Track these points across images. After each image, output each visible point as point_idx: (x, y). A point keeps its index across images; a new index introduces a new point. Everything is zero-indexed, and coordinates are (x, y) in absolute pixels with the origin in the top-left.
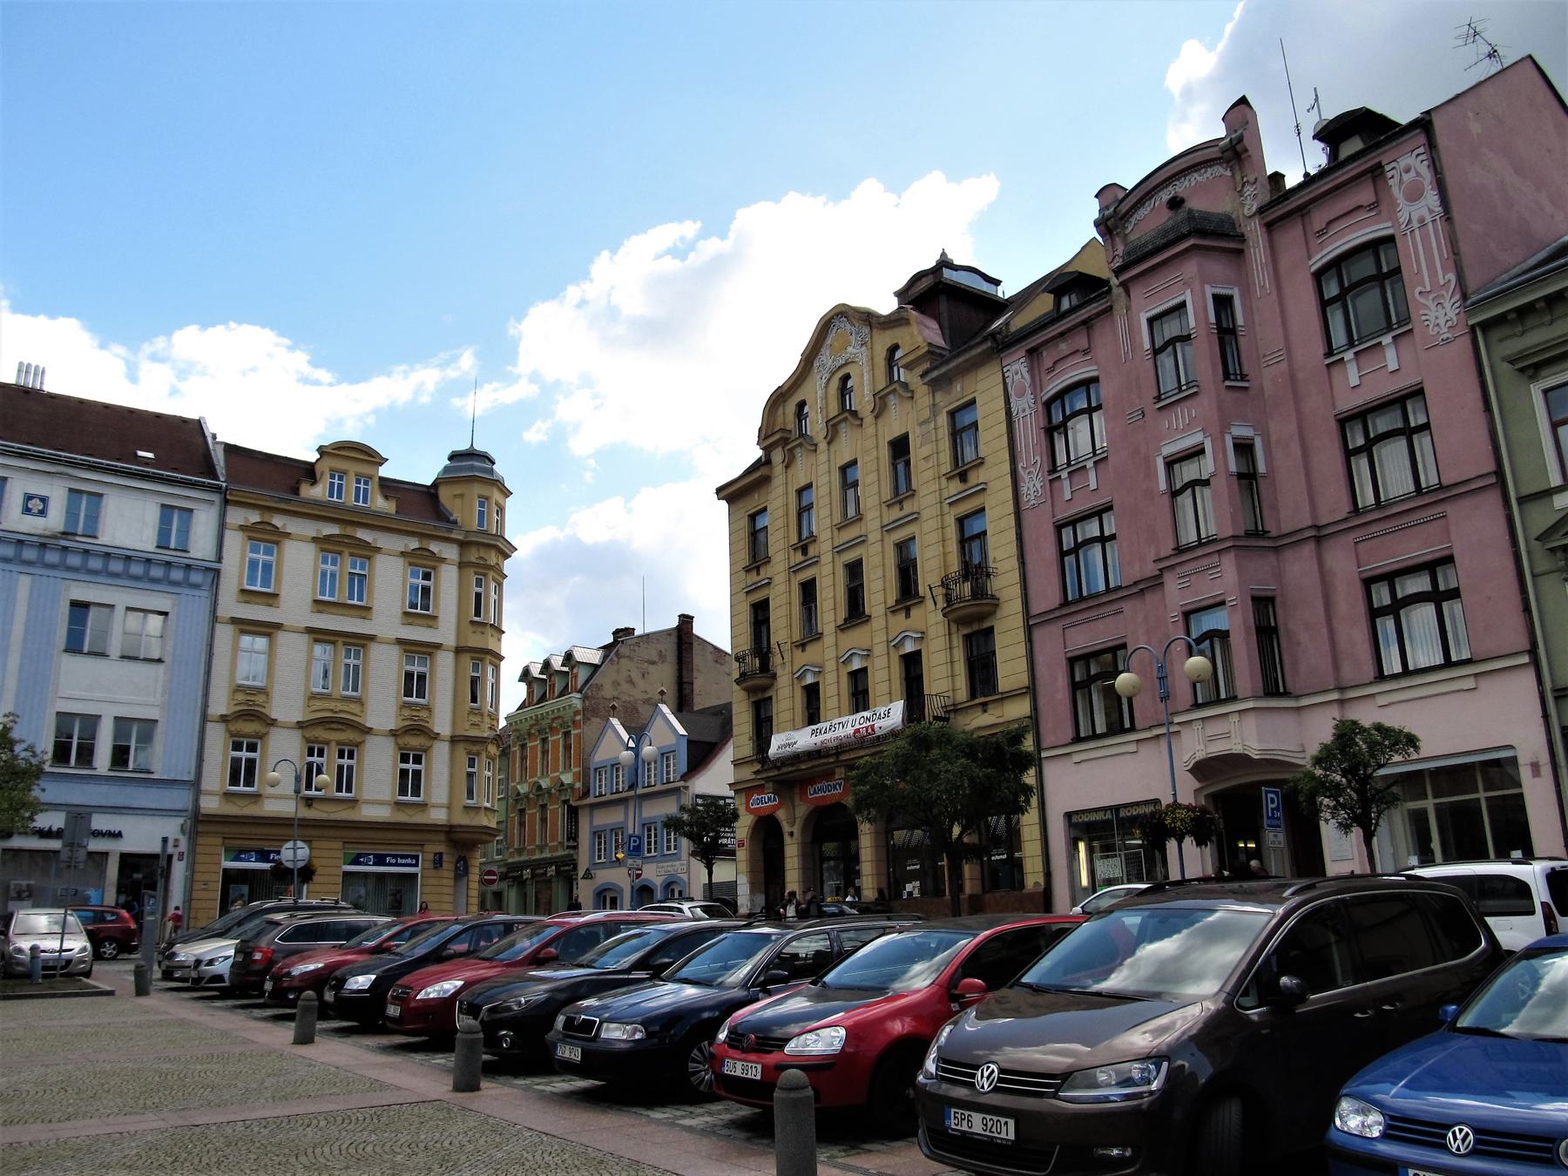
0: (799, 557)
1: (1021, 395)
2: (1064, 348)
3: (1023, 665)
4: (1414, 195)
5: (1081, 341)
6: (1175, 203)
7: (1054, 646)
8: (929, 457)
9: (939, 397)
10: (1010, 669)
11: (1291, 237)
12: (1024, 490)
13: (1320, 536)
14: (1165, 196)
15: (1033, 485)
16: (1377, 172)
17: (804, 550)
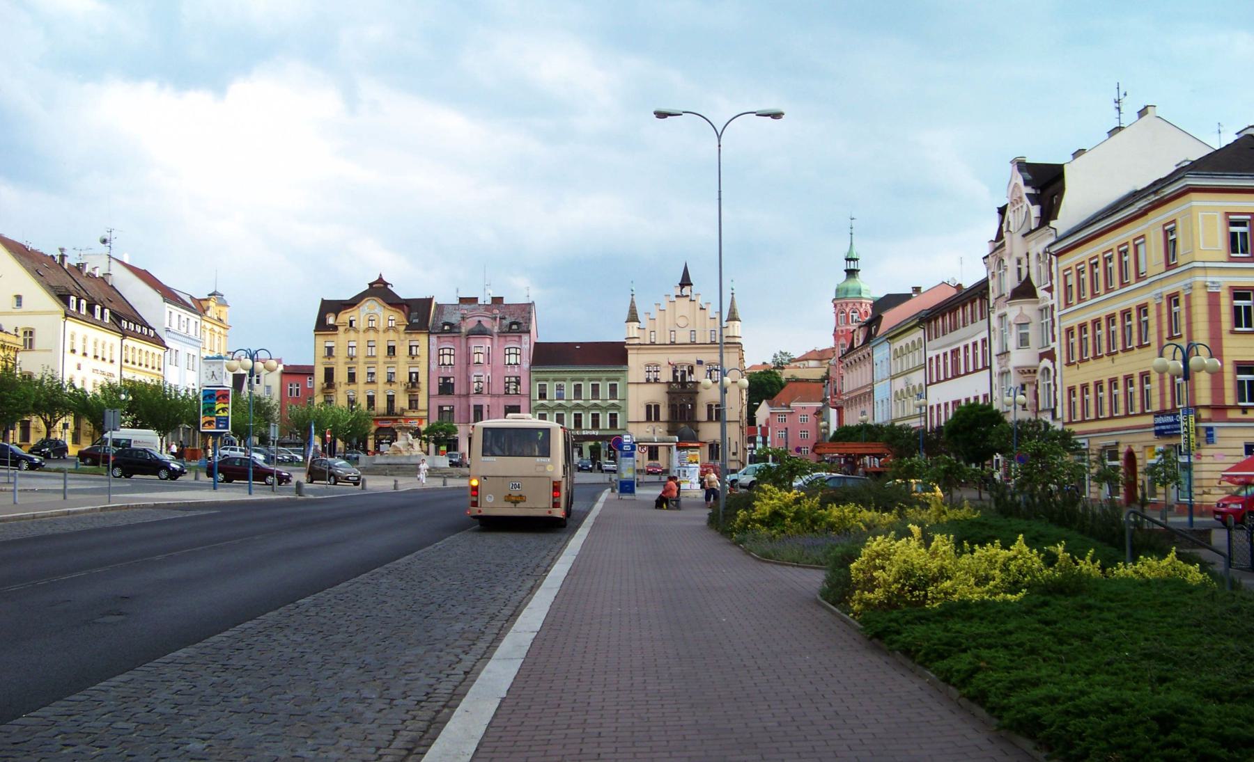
0: (349, 360)
1: (433, 345)
2: (446, 339)
3: (426, 405)
4: (525, 344)
5: (451, 339)
6: (479, 321)
7: (436, 403)
8: (402, 351)
9: (407, 335)
10: (422, 403)
11: (502, 339)
12: (431, 366)
13: (499, 396)
14: (478, 319)
15: (434, 367)
16: (520, 337)
17: (352, 359)
